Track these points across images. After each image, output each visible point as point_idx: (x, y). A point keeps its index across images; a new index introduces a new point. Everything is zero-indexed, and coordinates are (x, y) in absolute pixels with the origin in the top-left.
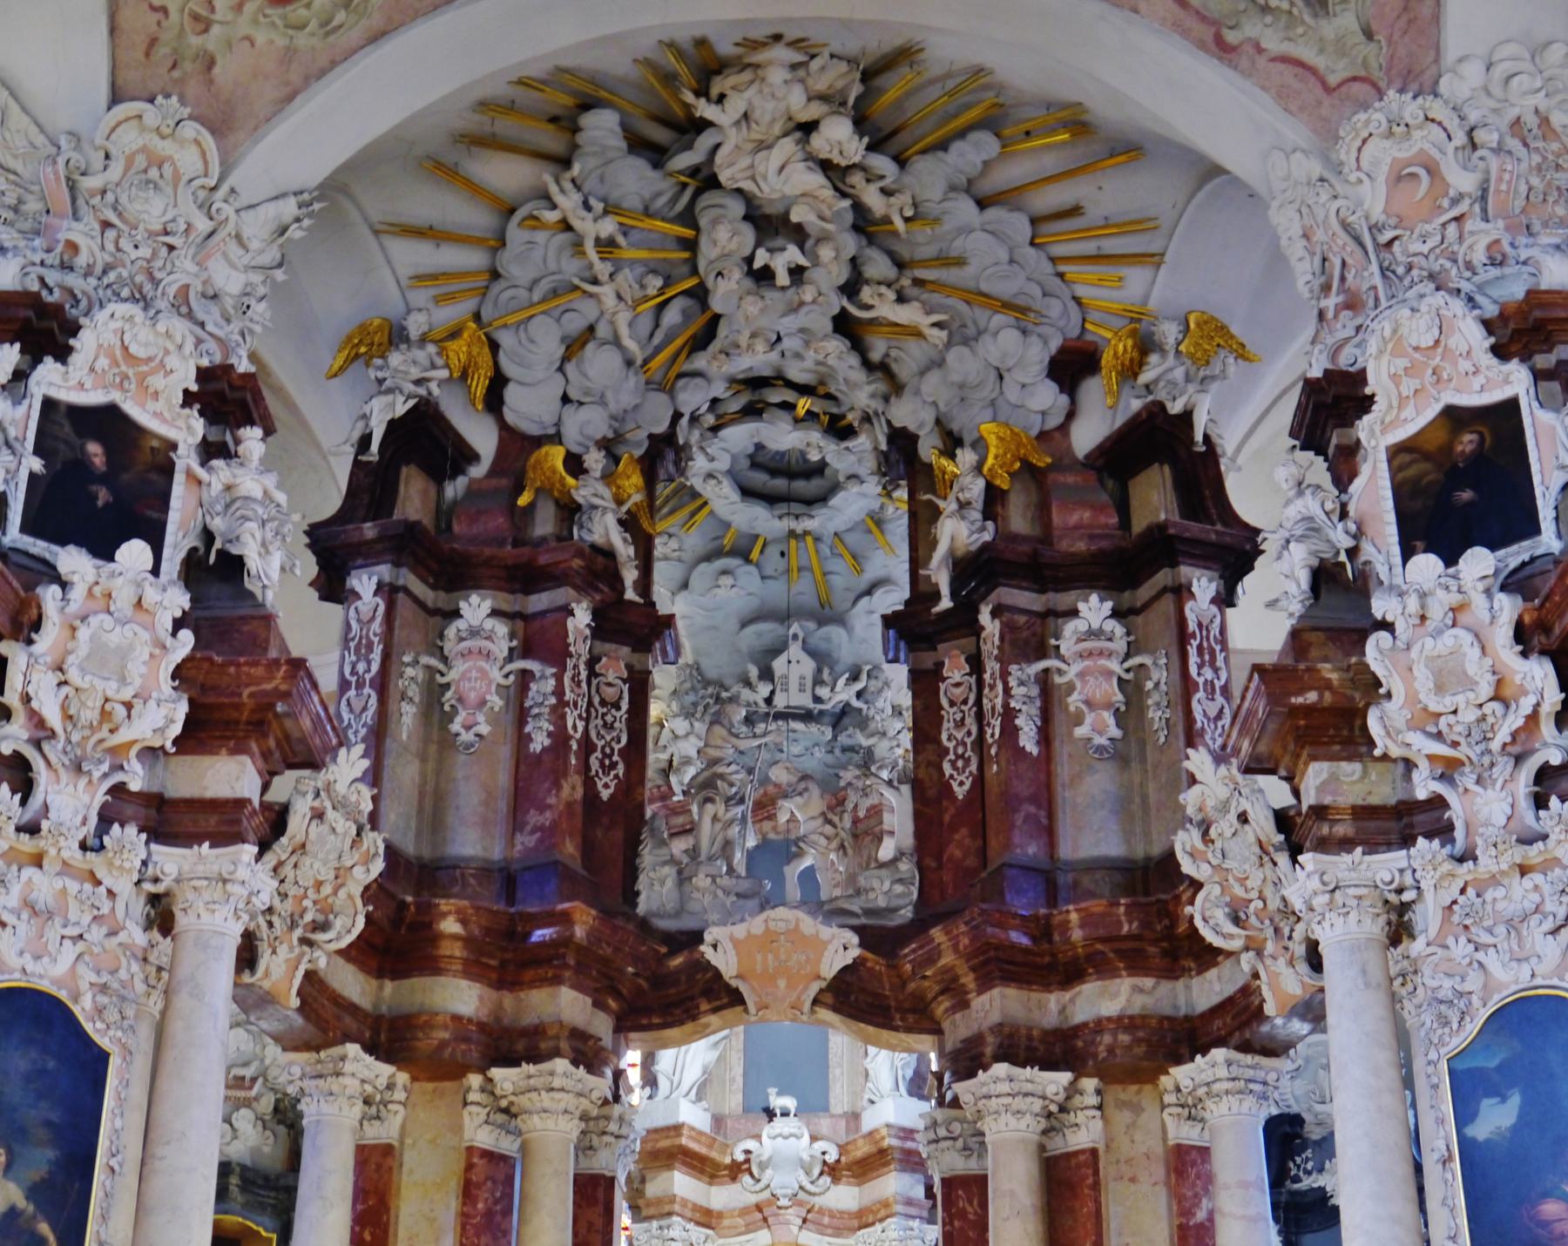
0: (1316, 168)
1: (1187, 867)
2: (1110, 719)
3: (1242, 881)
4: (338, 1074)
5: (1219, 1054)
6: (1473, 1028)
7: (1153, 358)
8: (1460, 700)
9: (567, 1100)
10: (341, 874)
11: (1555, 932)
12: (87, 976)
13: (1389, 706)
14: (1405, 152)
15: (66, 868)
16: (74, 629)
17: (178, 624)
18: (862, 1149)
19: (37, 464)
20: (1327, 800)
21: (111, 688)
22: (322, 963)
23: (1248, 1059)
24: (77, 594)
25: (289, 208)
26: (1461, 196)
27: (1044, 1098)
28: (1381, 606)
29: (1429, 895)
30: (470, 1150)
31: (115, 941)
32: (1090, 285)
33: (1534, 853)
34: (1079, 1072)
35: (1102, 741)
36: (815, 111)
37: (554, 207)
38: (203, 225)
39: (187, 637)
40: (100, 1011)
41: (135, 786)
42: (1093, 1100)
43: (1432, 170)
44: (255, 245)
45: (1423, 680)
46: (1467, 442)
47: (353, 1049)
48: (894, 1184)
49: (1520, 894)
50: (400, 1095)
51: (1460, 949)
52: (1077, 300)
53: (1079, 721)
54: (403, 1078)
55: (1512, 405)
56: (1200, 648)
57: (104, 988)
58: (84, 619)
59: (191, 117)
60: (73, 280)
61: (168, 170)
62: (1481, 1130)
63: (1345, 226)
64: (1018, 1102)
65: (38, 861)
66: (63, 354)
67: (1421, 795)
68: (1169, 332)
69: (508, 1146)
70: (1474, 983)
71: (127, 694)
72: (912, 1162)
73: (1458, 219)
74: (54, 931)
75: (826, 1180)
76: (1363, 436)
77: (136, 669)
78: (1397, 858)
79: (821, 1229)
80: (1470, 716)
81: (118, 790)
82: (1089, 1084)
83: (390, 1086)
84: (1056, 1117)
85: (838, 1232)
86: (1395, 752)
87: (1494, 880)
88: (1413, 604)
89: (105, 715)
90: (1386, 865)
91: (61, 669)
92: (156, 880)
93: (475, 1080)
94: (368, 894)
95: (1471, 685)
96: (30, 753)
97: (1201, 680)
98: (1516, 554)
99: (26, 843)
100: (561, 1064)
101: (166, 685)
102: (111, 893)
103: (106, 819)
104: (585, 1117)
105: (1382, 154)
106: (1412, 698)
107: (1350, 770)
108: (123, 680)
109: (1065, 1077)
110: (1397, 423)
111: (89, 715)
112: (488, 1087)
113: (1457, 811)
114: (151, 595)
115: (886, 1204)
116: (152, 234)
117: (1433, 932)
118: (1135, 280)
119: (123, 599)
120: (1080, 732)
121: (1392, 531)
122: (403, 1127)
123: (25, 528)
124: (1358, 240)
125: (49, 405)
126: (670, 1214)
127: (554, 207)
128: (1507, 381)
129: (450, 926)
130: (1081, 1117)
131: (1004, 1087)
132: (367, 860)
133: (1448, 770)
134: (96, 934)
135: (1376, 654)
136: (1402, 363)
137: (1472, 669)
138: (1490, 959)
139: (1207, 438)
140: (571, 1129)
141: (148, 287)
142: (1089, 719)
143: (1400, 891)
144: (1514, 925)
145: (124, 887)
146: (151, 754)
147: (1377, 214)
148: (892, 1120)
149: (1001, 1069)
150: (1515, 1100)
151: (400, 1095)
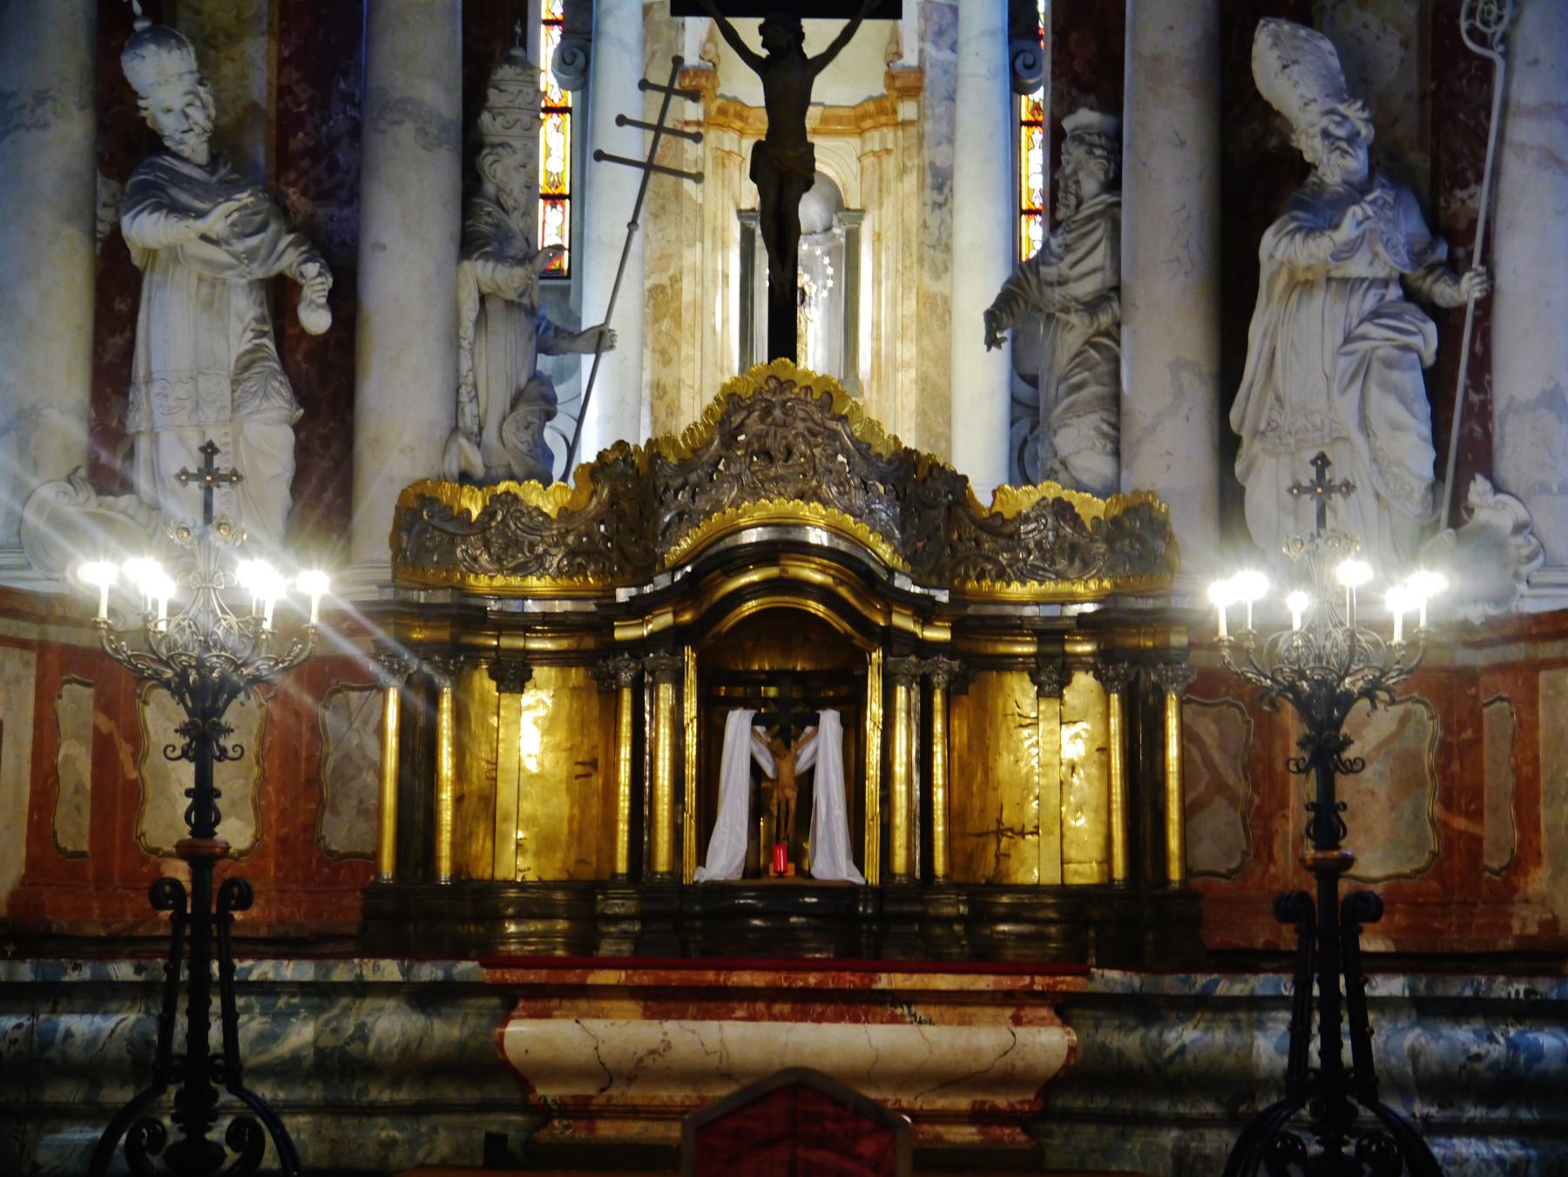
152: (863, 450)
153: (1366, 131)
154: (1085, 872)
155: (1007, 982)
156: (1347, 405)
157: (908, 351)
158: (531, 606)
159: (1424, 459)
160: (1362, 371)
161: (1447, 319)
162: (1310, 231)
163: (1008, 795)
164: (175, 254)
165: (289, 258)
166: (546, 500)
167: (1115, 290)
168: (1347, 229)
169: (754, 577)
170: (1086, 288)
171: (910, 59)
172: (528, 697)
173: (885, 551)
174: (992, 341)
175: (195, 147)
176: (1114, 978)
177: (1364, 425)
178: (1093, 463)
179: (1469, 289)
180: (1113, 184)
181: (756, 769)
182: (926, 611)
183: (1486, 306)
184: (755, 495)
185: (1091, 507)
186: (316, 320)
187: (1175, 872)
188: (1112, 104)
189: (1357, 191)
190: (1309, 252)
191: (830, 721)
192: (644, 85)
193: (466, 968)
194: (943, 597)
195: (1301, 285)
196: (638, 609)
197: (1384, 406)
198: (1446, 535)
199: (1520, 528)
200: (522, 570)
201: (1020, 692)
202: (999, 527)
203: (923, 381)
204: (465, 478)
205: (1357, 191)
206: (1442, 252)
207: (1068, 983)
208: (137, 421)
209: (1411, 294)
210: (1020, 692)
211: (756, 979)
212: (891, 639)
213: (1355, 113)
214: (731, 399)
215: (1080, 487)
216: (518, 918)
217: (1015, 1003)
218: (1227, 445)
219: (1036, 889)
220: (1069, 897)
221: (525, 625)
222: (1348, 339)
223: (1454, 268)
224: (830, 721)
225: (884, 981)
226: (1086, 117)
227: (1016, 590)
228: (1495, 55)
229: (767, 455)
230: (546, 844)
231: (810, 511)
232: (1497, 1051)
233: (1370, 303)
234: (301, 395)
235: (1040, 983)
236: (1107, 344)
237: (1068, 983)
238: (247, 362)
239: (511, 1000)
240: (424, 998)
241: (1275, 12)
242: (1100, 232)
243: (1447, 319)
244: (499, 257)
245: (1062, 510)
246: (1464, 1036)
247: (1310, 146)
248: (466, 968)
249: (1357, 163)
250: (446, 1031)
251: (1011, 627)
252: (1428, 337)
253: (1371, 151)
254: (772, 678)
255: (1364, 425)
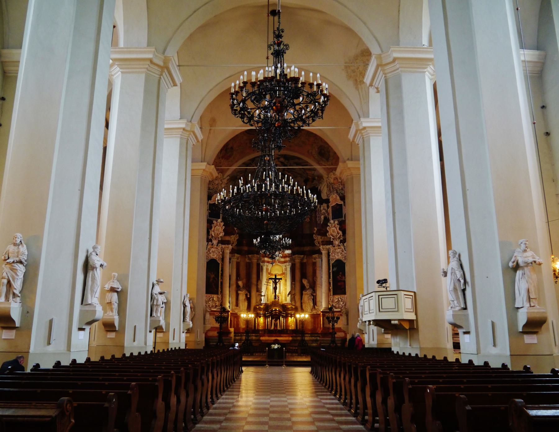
0: (327, 176)
1: (314, 238)
2: (309, 219)
3: (319, 240)
4: (235, 256)
5: (317, 255)
6: (334, 261)
7: (315, 181)
8: (334, 233)
9: (255, 258)
10: (234, 239)
11: (341, 254)
12: (217, 257)
13: (329, 233)
14: (335, 177)
15: (215, 248)
16: (215, 228)
17: (223, 226)
18: (284, 255)
19: (210, 211)
20: (324, 240)
21: (218, 232)
22: (233, 247)
23: (320, 255)
24: (215, 224)
25: (228, 177)
26: (339, 182)
27: (301, 258)
28: (329, 224)
29: (331, 250)
30: (247, 262)
31: (219, 254)
32: (308, 172)
33: (340, 247)
34: (304, 255)
35: (308, 221)
36: (279, 157)
37: (252, 165)
38: (221, 182)
39: (224, 227)
40: (219, 260)
41: (220, 240)
42: (305, 258)
43: (337, 179)
44: (225, 182)
45: (331, 231)
46: (338, 207)
47: (236, 254)
48: (288, 259)
49: (339, 250)
50: (240, 257)
51: (333, 254)
52: (307, 174)
53: (306, 219)
54: (240, 256)
55: (342, 204)
56: (318, 213)
57: (219, 258)
58: (215, 226)
59: (220, 172)
60: (211, 191)
61: (218, 178)
62: (334, 270)
63: (329, 183)
64: (299, 258)
65: (213, 247)
66: (211, 199)
67: (331, 240)
68: (316, 178)
69: (250, 261)
70: (334, 258)
71: (219, 232)
72: (289, 257)
73: (339, 184)
74: (215, 253)
75: (281, 258)
76: (329, 205)
77: (220, 230)
78: (329, 246)
79: (280, 263)
80: (335, 235)
81: (219, 240)
82: (305, 256)
83: (239, 256)
84: (302, 259)
85: (282, 263)
86: (329, 237)
87: (337, 249)
88: (331, 224)
89: (217, 234)
90: (328, 247)
91: (214, 231)
92: (222, 248)
93: (247, 256)
94: (237, 240)
95: (335, 232)
96: (212, 238)
97: (318, 216)
98: (340, 219)
99: (212, 246)
100: (255, 255)
101: (222, 231)
102: (219, 250)
103: (218, 243)
104: (257, 259)
105: (333, 176)
106: (331, 232)
107: (326, 237)
108: (219, 232)
109: (303, 256)
110: (333, 204)
111: (216, 234)
112: (248, 256)
113: (334, 242)
114: (221, 224)
115: (287, 261)
116: (217, 184)
117: (331, 252)
118: (313, 172)
119: (219, 224)
120: (306, 220)
121: (331, 214)
122: (240, 260)
123: (209, 217)
124: (330, 184)
125: (209, 204)
126: (265, 262)
127: (252, 165)
128: (341, 202)
129: (244, 242)
130: (305, 259)
131: (297, 257)
132: (237, 237)
133: (333, 239)
134: (218, 253)
135: (328, 228)
136: (333, 199)
137: (335, 231)
138: (336, 256)
139: (320, 190)
140: (256, 260)
141: (217, 190)
142: (307, 219)
143: (329, 249)
144: (338, 253)
145: (220, 249)
146: (221, 237)
147: (332, 182)
148: (287, 253)
149: (297, 255)
150: (336, 268)
151: (240, 257)
152: (280, 305)
153: (309, 285)
154: (293, 329)
155: (289, 335)
156: (308, 301)
157: (284, 292)
158: (261, 313)
159: (312, 304)
160: (309, 300)
161: (314, 296)
162: (305, 291)
163: (289, 324)
164: (241, 293)
165: (247, 293)
166: (262, 307)
167: (295, 294)
168: (307, 292)
169: (274, 312)
170: (294, 293)
171: (284, 272)
172: (261, 318)
173: (281, 310)
174: (288, 296)
175: (242, 287)
176: (294, 335)
177: (309, 303)
178: (294, 304)
179: (315, 294)
180: (295, 287)
181: (274, 323)
182: (284, 314)
183: (316, 296)
184: (274, 307)
185: (293, 307)
186: (249, 296)
187: (298, 329)
188: (295, 282)
189: (309, 289)
190: (306, 293)
191: (278, 320)
192: (267, 280)
193: (258, 335)
194: (285, 313)
195: (305, 294)
196: (267, 314)
197: (310, 301)
198: (314, 309)
199: (318, 308)
200: (261, 311)
201: (290, 318)
202: (288, 308)
203: (285, 294)
204: (257, 305)
205: (309, 289)
206: (314, 292)
207: (292, 335)
208: (239, 303)
209: (311, 294)
210: (290, 318)
211: (274, 335)
212: (282, 315)
213: (308, 284)
214: (273, 302)
215: (293, 306)
216: (261, 331)
217: (289, 336)
218: (301, 303)
219: (291, 330)
220: (292, 330)
221: (261, 314)
222: (308, 297)
223: (314, 293)
224: (278, 320)
225: (282, 335)
226: (293, 283)
227: (289, 312)
228: (316, 281)
229: (275, 305)
230: (262, 327)
231: (277, 308)
232: (315, 339)
233: (309, 295)
234: (248, 301)
235: (290, 335)
236: (294, 297)
237: (292, 335)
238: (245, 299)
239: (261, 336)
240: (256, 336)
241: (304, 278)
242: (294, 290)
243: (314, 296)
244: (259, 292)
245: (292, 307)
246: (313, 338)
247: (306, 286)
248: (258, 335)
249: (308, 287)
250: (257, 338)
251: (289, 314)
252: (313, 297)
253: (309, 286)
254: (275, 317)
255: (309, 303)
